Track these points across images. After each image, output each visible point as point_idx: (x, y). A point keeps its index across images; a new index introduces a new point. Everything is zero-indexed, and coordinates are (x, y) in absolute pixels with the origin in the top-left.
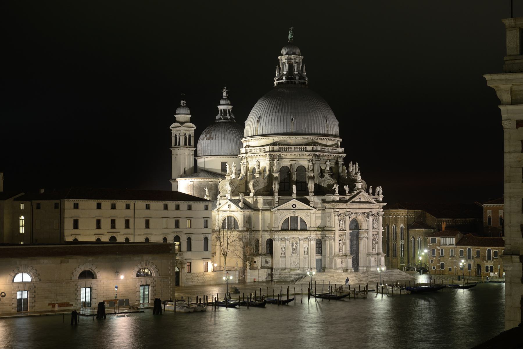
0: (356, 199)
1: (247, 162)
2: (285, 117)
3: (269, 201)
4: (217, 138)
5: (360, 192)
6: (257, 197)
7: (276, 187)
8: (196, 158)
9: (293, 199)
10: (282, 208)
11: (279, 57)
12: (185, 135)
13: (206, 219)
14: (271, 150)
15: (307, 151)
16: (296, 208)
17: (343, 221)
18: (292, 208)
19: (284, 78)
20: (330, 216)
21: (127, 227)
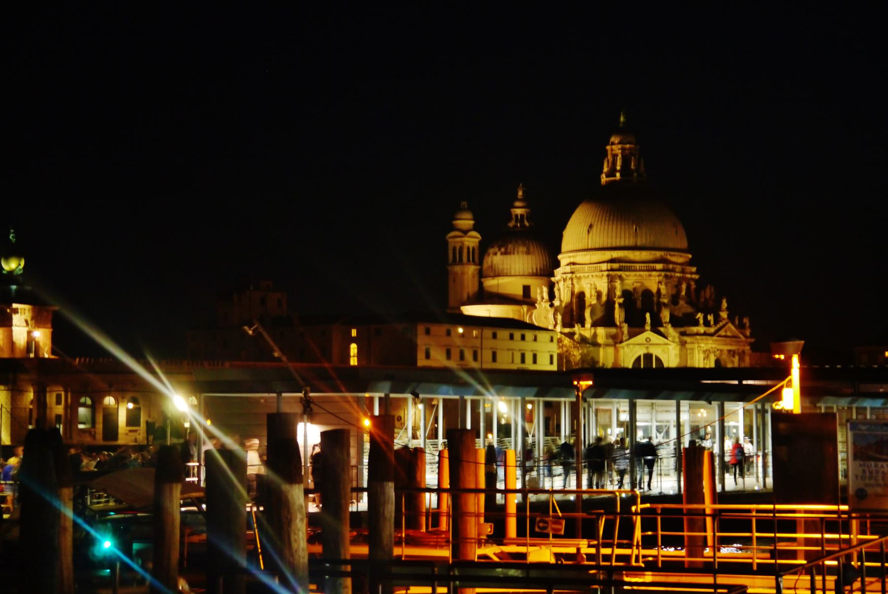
0: (722, 333)
1: (572, 284)
2: (606, 227)
3: (612, 333)
4: (516, 253)
5: (726, 324)
6: (597, 329)
7: (619, 315)
8: (483, 280)
9: (647, 330)
10: (633, 343)
11: (608, 147)
12: (468, 248)
13: (551, 353)
14: (609, 268)
15: (655, 270)
16: (651, 343)
17: (707, 361)
18: (645, 342)
19: (618, 175)
20: (692, 353)
21: (475, 358)
